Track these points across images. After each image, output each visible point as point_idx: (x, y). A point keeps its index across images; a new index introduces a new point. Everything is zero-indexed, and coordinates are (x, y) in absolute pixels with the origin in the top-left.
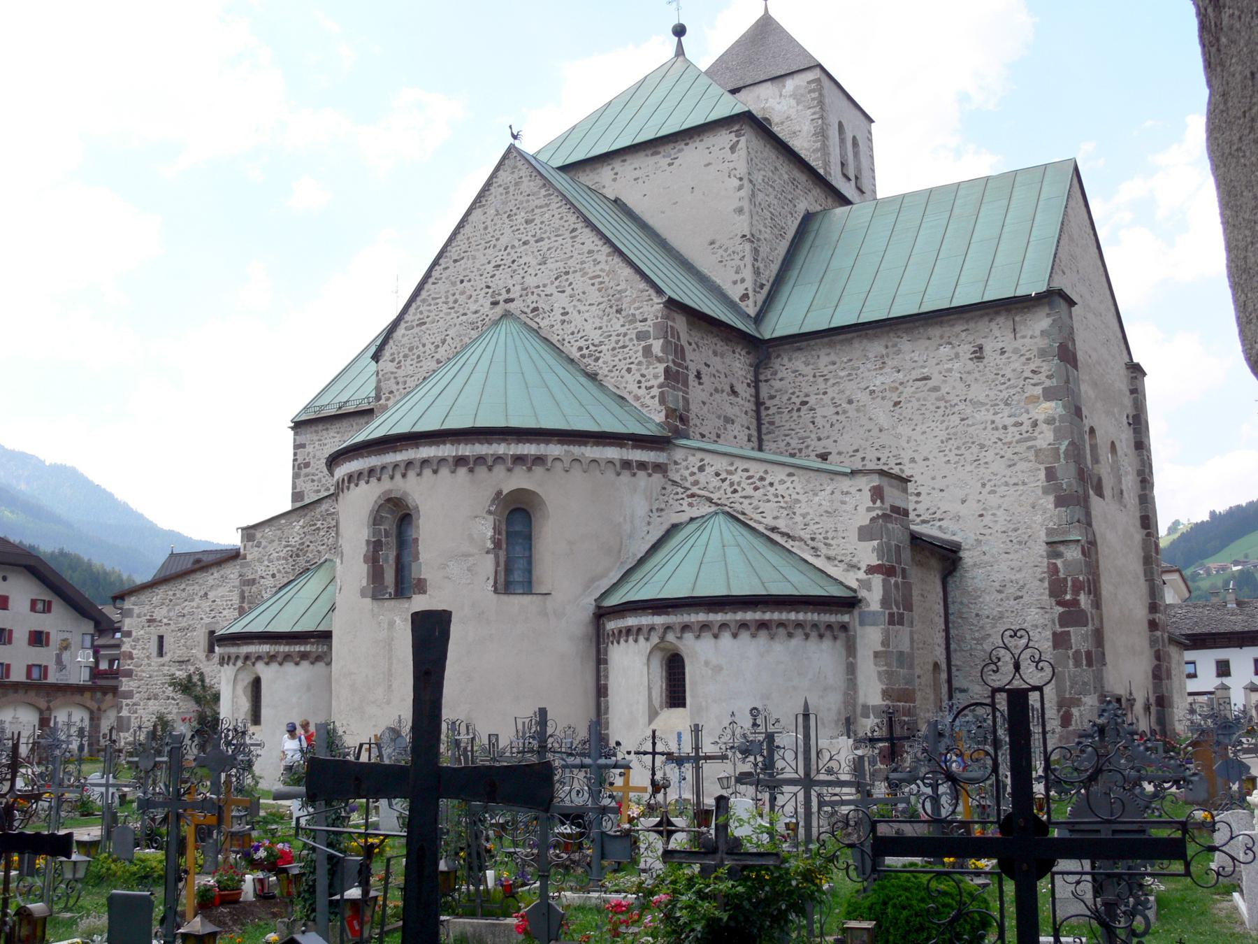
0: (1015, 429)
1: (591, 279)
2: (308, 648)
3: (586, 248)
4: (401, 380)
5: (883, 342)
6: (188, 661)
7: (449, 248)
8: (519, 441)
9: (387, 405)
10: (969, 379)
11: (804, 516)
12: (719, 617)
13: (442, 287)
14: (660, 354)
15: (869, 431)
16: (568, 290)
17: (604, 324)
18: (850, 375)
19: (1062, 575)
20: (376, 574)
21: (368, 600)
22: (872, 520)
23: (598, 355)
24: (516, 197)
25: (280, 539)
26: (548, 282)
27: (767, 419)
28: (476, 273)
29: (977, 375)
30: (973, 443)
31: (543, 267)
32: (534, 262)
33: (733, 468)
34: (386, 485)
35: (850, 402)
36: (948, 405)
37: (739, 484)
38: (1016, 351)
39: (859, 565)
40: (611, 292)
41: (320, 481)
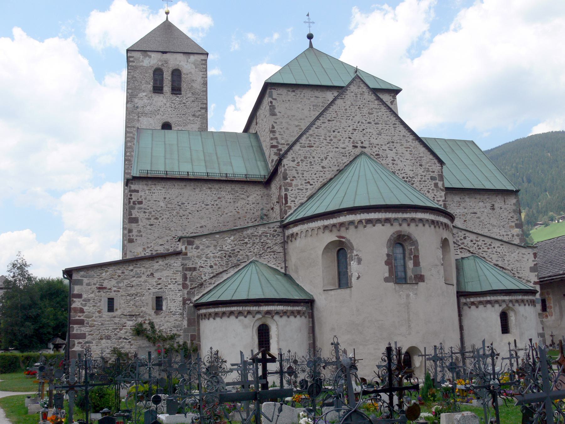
0: (507, 237)
1: (405, 148)
4: (300, 172)
6: (139, 315)
7: (325, 113)
10: (490, 216)
11: (508, 261)
12: (526, 298)
13: (322, 131)
14: (442, 188)
17: (414, 170)
21: (391, 285)
22: (535, 265)
24: (361, 100)
26: (383, 144)
28: (342, 129)
32: (375, 133)
33: (478, 239)
34: (396, 228)
37: (481, 246)
38: (505, 209)
40: (416, 156)
41: (150, 213)
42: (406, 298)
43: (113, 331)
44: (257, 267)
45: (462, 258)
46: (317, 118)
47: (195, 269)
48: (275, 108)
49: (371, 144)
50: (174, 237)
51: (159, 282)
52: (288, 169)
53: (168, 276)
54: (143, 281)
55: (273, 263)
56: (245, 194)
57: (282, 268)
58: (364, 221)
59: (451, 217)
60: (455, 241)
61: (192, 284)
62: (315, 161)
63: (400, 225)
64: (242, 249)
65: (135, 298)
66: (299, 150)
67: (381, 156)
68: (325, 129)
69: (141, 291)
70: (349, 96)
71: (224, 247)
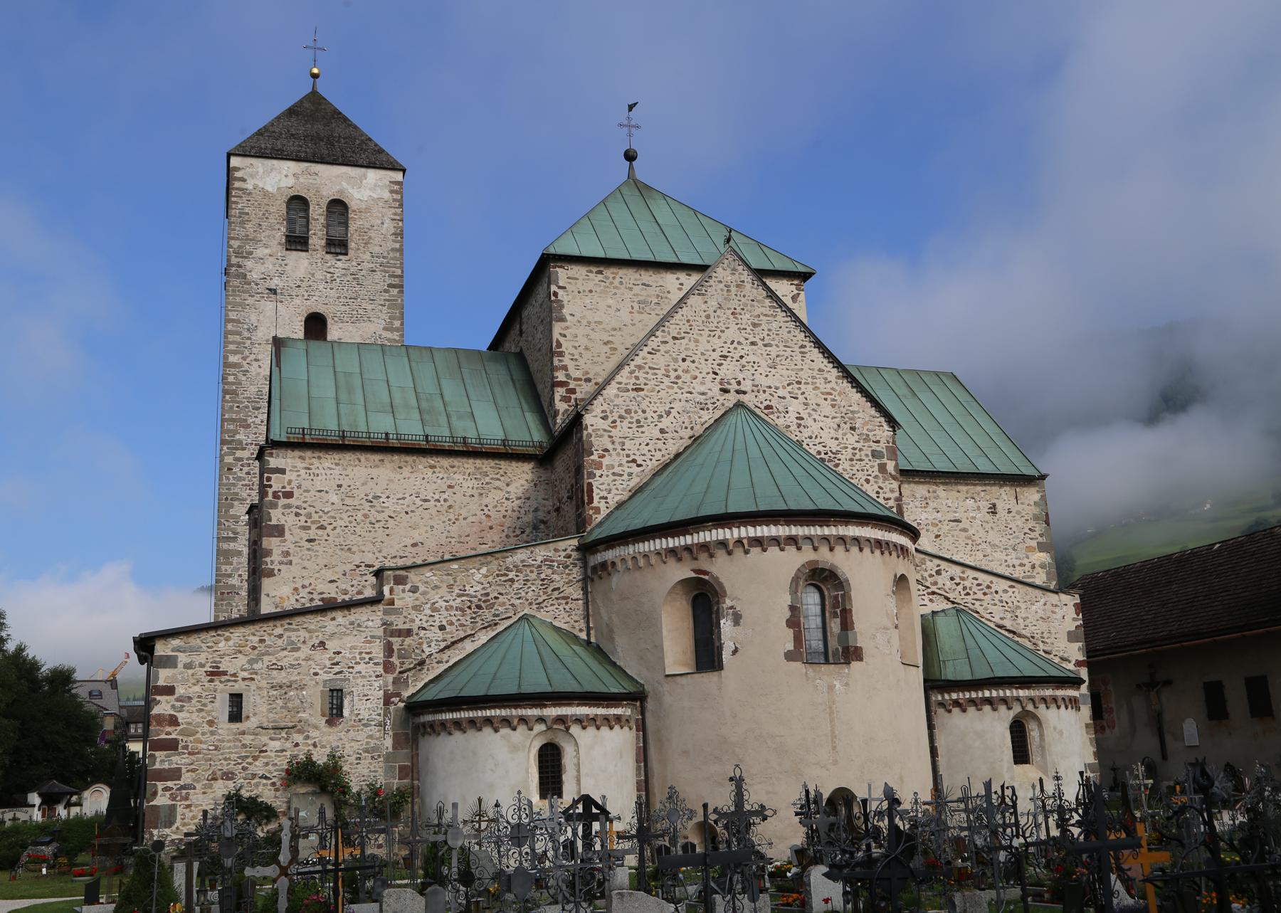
1: (822, 393)
4: (617, 440)
5: (926, 487)
6: (293, 727)
9: (601, 463)
11: (1025, 619)
12: (1060, 693)
13: (660, 361)
14: (893, 473)
17: (840, 437)
23: (838, 462)
26: (780, 385)
29: (991, 524)
32: (763, 364)
33: (965, 576)
34: (807, 555)
36: (974, 543)
40: (844, 410)
42: (828, 693)
43: (240, 761)
44: (533, 630)
45: (933, 612)
46: (652, 333)
47: (409, 633)
48: (563, 306)
49: (757, 386)
50: (358, 566)
51: (335, 661)
52: (593, 434)
56: (502, 478)
57: (581, 630)
59: (914, 534)
60: (920, 579)
61: (403, 663)
62: (646, 419)
64: (504, 592)
65: (286, 693)
66: (617, 396)
67: (775, 409)
68: (667, 355)
69: (298, 678)
70: (715, 290)
71: (467, 588)
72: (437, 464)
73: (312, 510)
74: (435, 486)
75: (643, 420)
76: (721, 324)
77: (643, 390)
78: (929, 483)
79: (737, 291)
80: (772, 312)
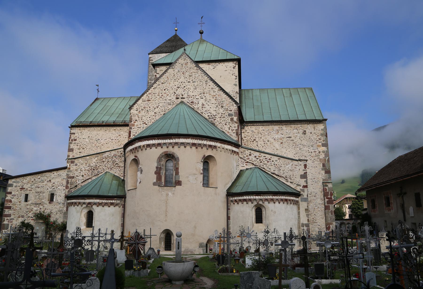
0: (314, 153)
1: (212, 96)
2: (113, 201)
3: (211, 87)
5: (278, 126)
6: (40, 204)
8: (210, 141)
10: (302, 139)
13: (157, 91)
14: (236, 121)
15: (274, 149)
16: (204, 98)
17: (217, 110)
18: (268, 134)
19: (327, 191)
20: (159, 178)
21: (157, 187)
22: (304, 173)
23: (215, 118)
24: (185, 68)
25: (86, 164)
27: (244, 143)
30: (303, 155)
31: (195, 90)
32: (192, 88)
33: (261, 156)
34: (165, 149)
35: (268, 141)
36: (296, 145)
37: (262, 160)
38: (315, 133)
39: (301, 185)
40: (220, 101)
42: (166, 196)
43: (26, 213)
47: (73, 177)
52: (133, 115)
53: (58, 182)
54: (45, 184)
55: (118, 173)
57: (122, 176)
58: (145, 146)
61: (71, 186)
62: (150, 109)
63: (167, 147)
64: (101, 165)
65: (39, 194)
66: (142, 103)
67: (194, 103)
69: (43, 190)
70: (177, 66)
71: (91, 164)
72: (116, 129)
73: (81, 144)
74: (115, 135)
75: (149, 110)
76: (178, 77)
77: (150, 100)
78: (279, 125)
79: (185, 66)
80: (197, 71)
